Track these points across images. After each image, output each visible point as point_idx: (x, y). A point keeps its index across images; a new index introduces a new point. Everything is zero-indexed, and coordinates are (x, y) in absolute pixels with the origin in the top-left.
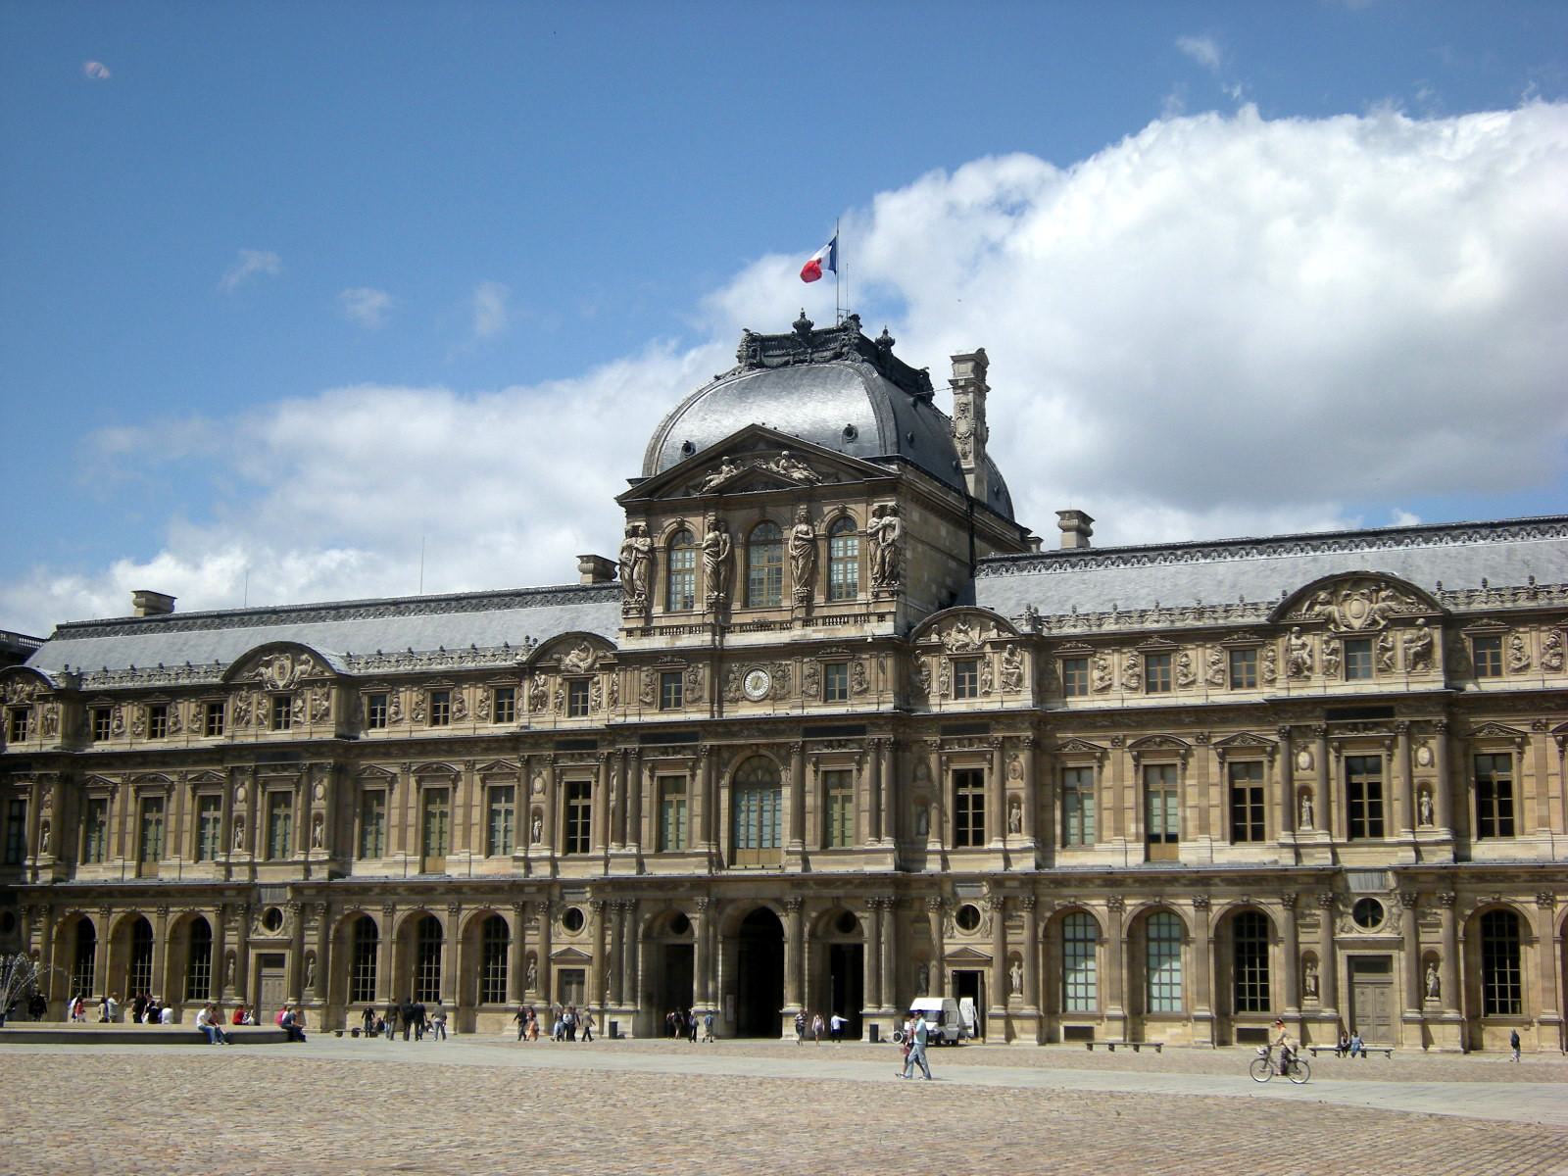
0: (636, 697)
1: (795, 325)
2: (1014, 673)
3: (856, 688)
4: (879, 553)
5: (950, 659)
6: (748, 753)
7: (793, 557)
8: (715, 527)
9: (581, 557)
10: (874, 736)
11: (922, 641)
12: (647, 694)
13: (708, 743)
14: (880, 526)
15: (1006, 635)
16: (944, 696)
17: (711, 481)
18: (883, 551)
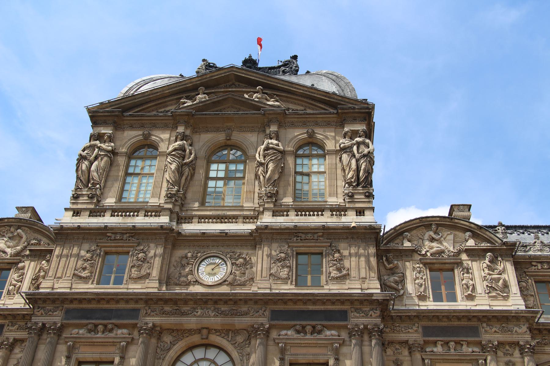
0: (70, 272)
1: (245, 62)
2: (499, 279)
3: (334, 274)
4: (354, 162)
5: (425, 264)
6: (196, 339)
7: (261, 164)
8: (184, 137)
9: (17, 208)
10: (358, 320)
11: (392, 245)
12: (84, 269)
13: (151, 320)
14: (354, 142)
15: (484, 245)
16: (422, 298)
17: (185, 103)
18: (357, 161)
